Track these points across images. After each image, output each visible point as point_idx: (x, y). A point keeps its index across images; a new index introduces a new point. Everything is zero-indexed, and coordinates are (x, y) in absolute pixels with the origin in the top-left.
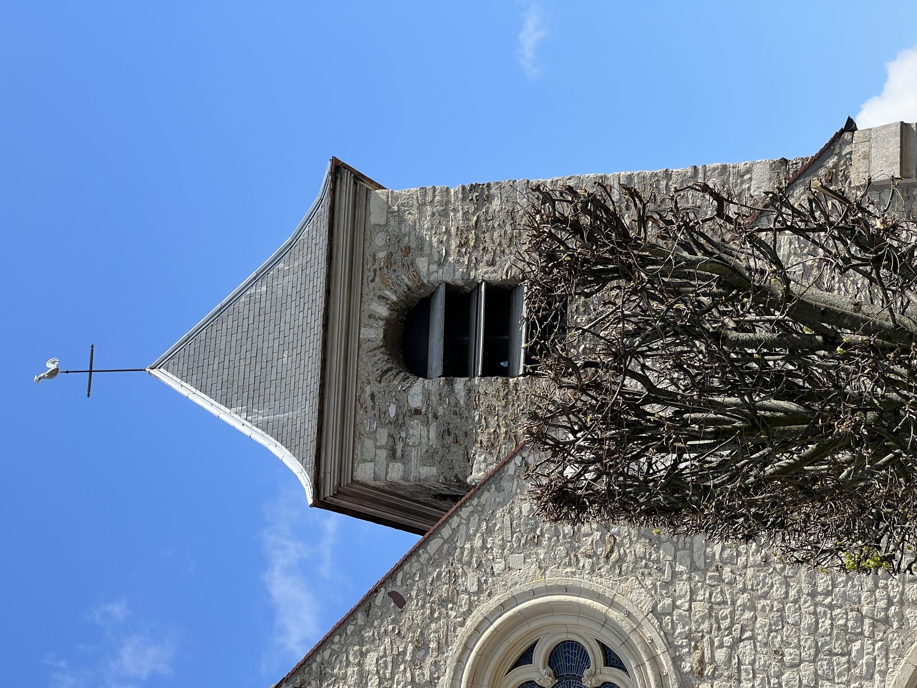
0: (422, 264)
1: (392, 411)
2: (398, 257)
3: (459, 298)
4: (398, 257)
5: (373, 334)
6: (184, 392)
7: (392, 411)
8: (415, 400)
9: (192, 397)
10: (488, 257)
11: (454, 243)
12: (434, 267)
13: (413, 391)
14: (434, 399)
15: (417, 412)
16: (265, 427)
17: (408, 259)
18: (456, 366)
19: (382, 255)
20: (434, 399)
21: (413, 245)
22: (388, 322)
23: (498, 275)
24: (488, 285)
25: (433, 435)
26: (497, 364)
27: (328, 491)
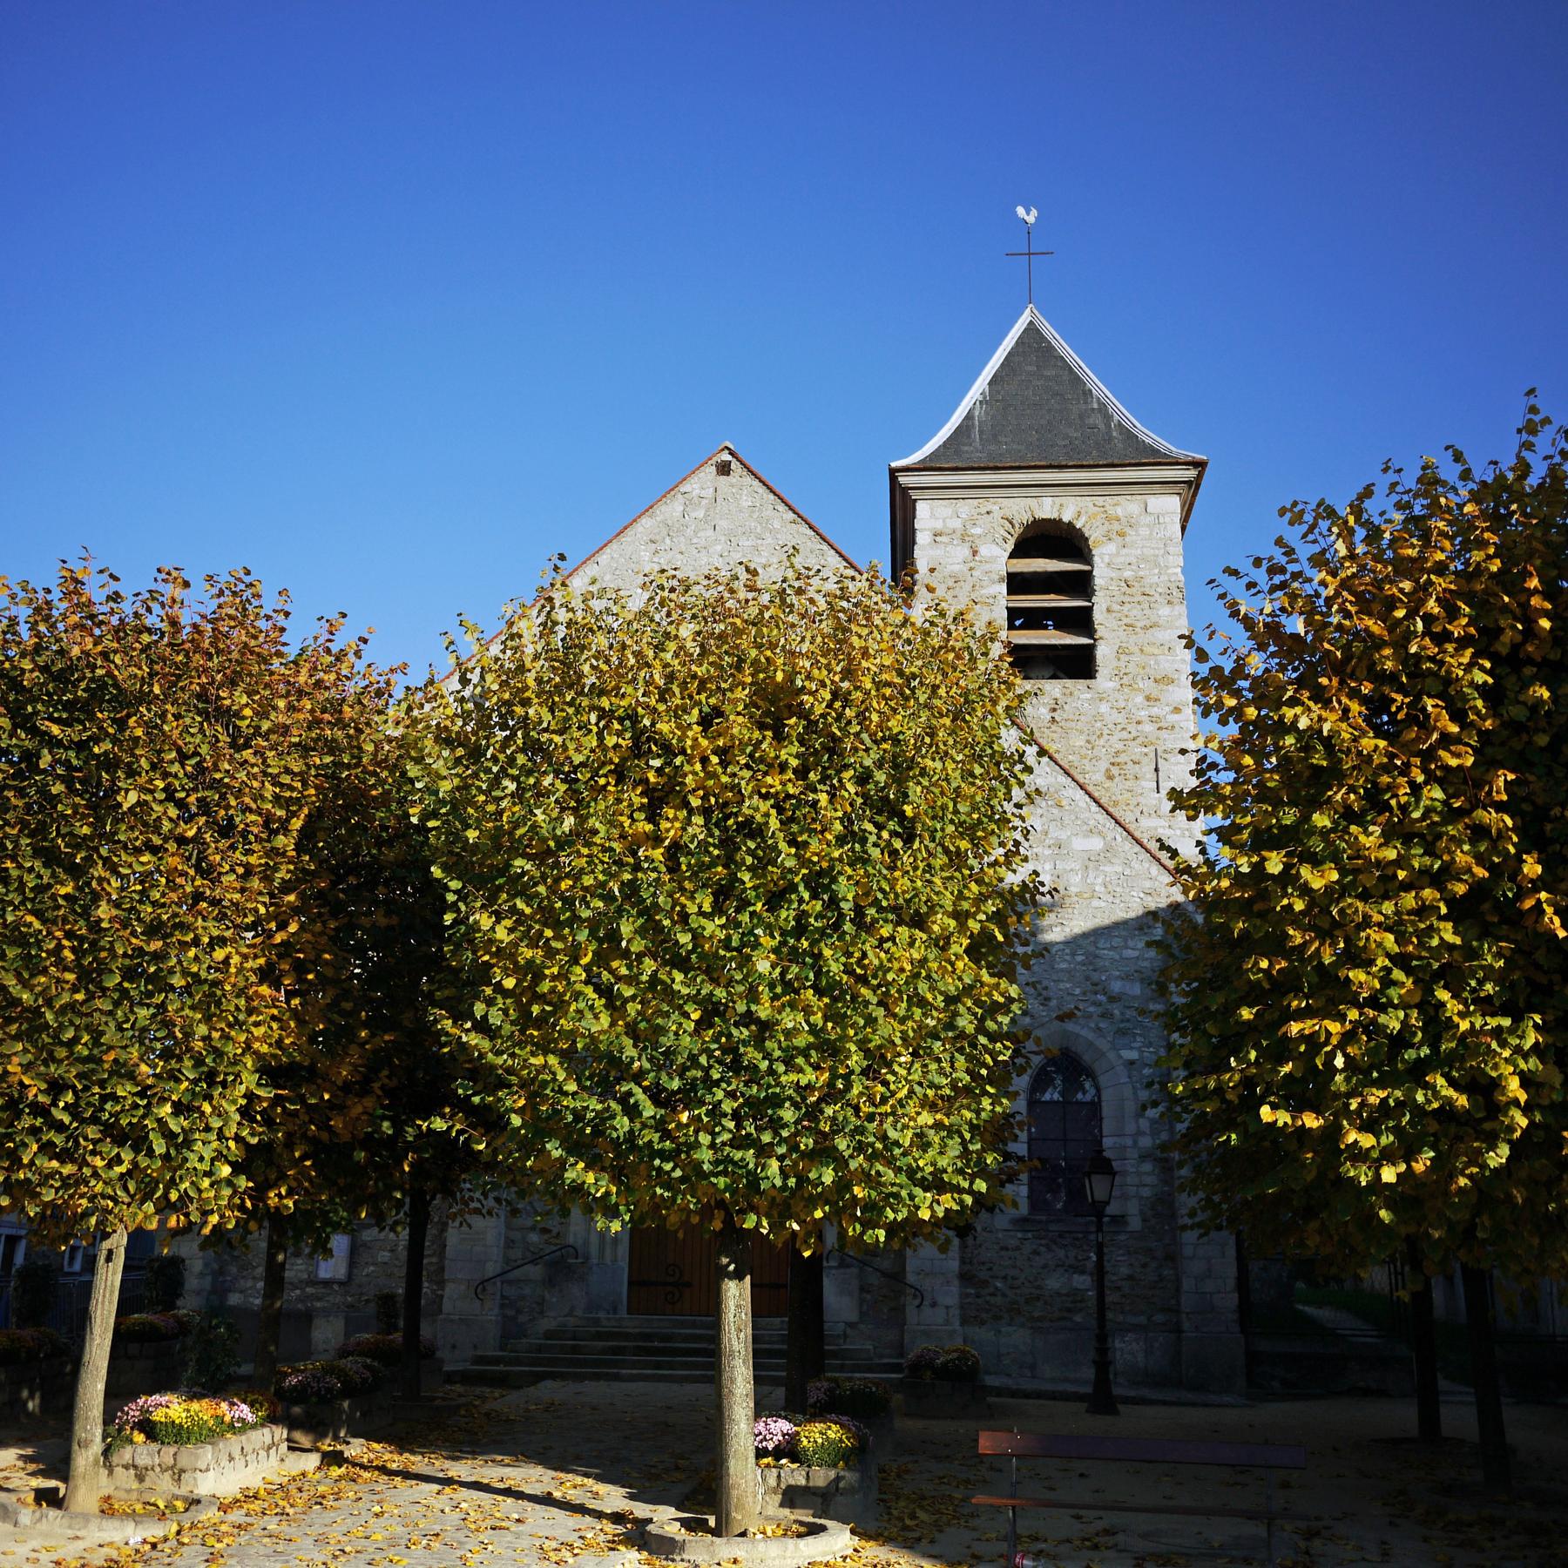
0: (1111, 548)
1: (977, 531)
2: (1116, 526)
3: (1081, 584)
4: (1116, 526)
5: (1047, 507)
6: (1005, 343)
7: (977, 531)
8: (985, 550)
9: (1001, 348)
10: (1116, 607)
11: (1128, 574)
12: (1107, 559)
13: (994, 546)
14: (987, 567)
15: (975, 553)
16: (969, 416)
17: (1114, 536)
18: (1016, 584)
19: (1119, 511)
20: (987, 567)
21: (1128, 539)
22: (1057, 523)
23: (1098, 616)
24: (1089, 610)
25: (956, 568)
26: (1020, 618)
27: (903, 480)
